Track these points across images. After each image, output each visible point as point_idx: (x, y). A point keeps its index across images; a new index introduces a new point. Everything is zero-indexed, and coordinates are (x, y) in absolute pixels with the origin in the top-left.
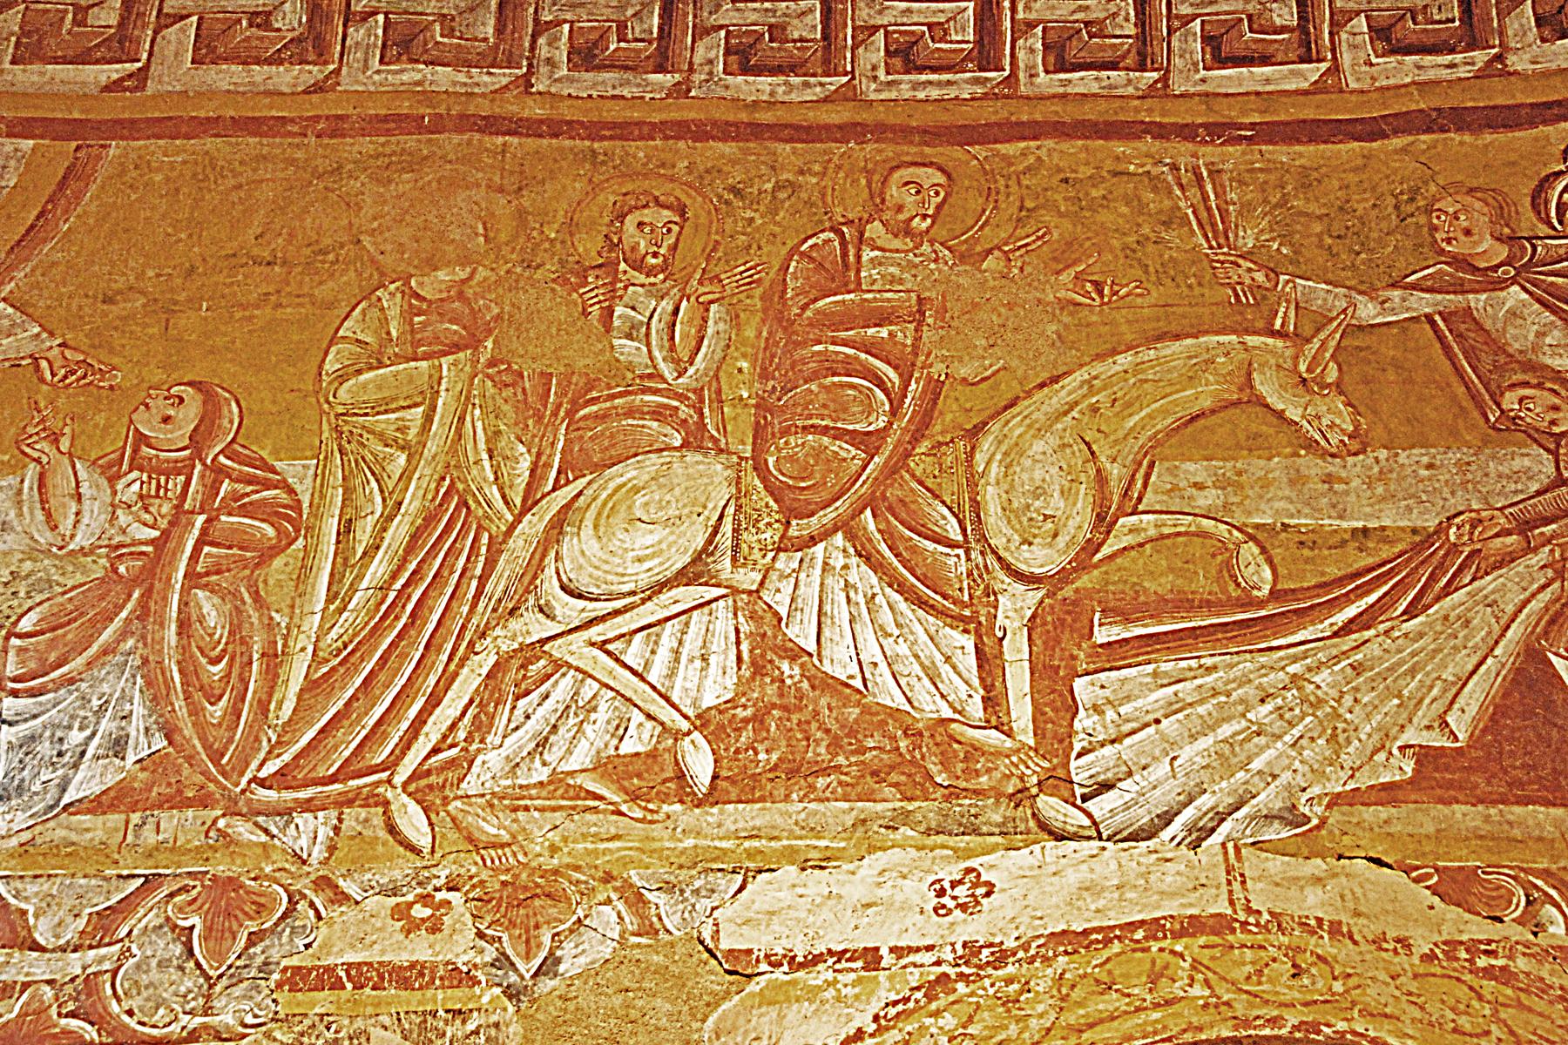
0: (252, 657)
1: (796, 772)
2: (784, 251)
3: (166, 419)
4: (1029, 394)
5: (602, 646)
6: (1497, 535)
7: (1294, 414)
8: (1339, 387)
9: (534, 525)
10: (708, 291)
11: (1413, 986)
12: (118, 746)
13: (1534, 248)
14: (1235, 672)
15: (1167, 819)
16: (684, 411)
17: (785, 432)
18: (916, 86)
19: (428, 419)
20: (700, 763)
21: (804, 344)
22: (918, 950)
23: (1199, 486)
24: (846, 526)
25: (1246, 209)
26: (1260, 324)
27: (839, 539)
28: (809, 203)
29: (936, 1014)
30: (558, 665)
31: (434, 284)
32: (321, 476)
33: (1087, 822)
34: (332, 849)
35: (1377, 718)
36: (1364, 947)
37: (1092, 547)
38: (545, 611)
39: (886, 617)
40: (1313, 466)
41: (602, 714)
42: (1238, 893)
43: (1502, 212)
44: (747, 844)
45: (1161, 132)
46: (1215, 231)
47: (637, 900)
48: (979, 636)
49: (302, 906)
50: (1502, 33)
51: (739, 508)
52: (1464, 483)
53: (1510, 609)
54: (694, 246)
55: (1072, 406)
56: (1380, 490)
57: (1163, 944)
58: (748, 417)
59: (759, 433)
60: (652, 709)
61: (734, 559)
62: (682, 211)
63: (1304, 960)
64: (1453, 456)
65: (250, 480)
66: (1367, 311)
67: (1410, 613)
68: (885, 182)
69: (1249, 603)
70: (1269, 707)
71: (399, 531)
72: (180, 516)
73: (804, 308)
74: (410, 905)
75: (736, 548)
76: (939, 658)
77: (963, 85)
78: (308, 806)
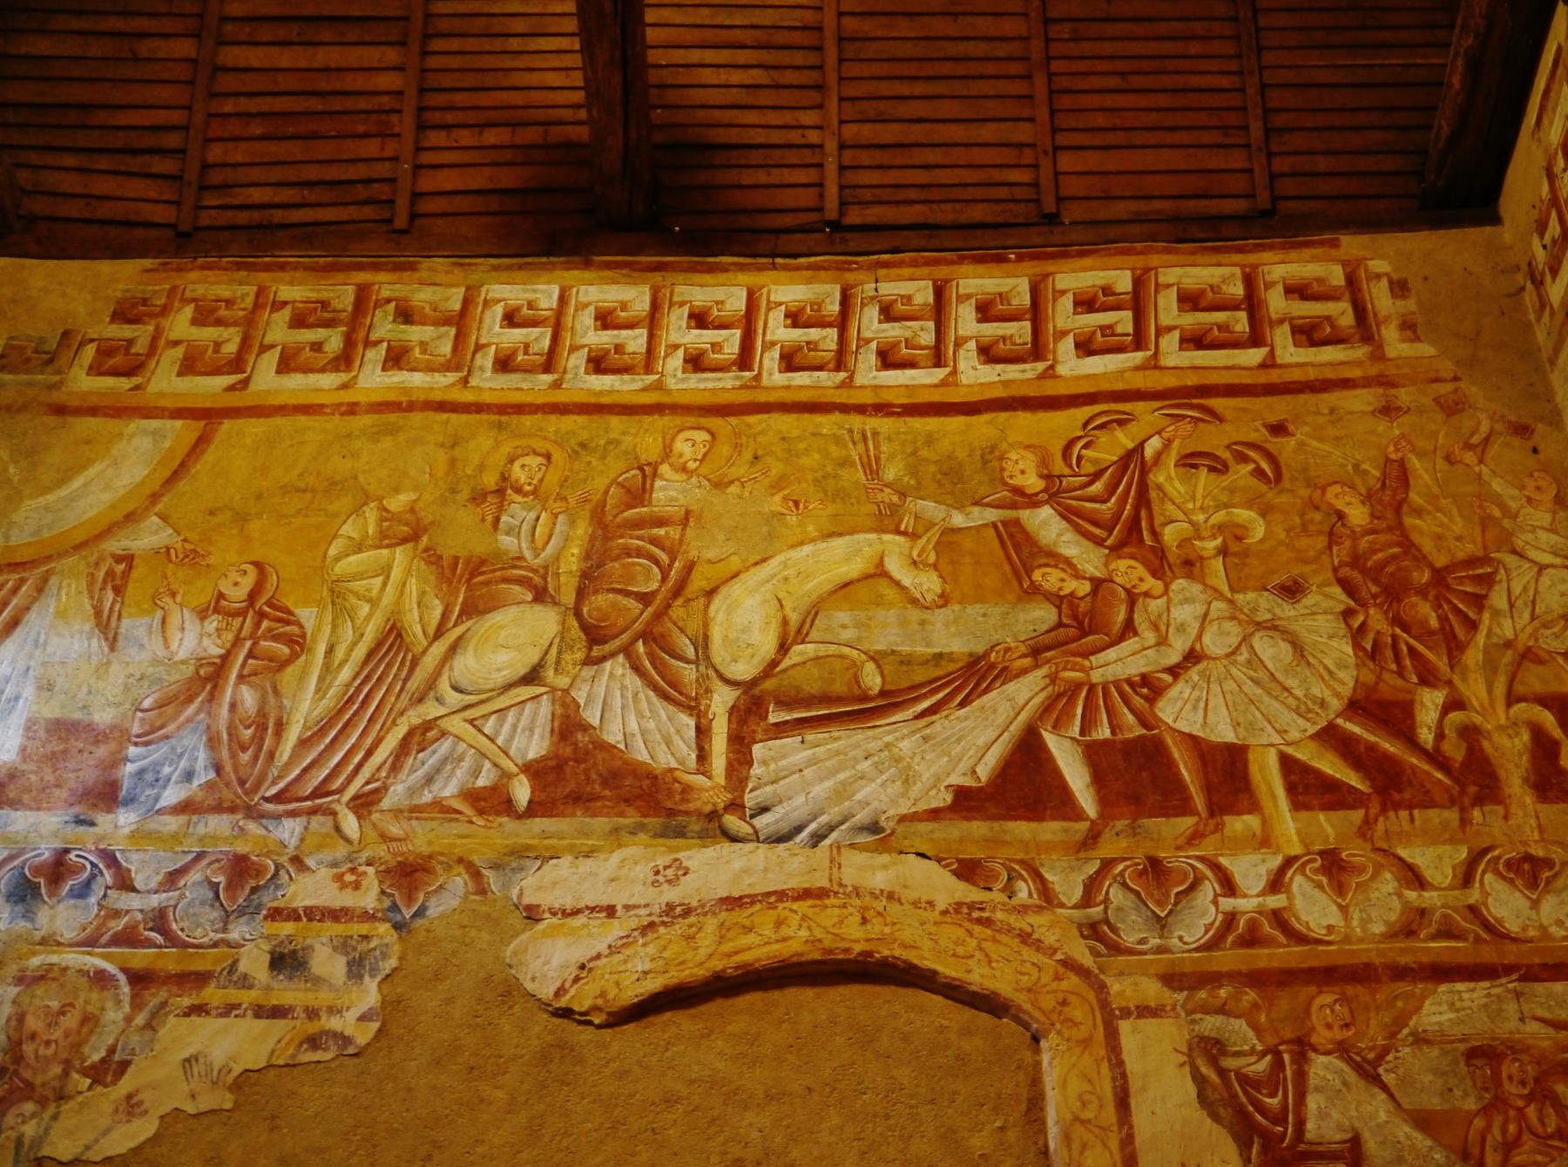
0: (268, 724)
1: (580, 800)
2: (607, 481)
3: (236, 584)
4: (747, 569)
5: (471, 722)
7: (906, 582)
8: (935, 566)
9: (439, 648)
10: (558, 506)
11: (933, 929)
12: (189, 776)
14: (853, 740)
15: (799, 829)
16: (537, 580)
17: (596, 592)
18: (700, 380)
19: (385, 584)
20: (522, 792)
21: (611, 539)
22: (638, 907)
23: (844, 626)
24: (627, 651)
25: (892, 456)
26: (892, 527)
27: (621, 658)
28: (626, 453)
29: (644, 945)
30: (443, 734)
31: (397, 503)
32: (320, 618)
33: (750, 831)
34: (302, 840)
35: (934, 769)
36: (907, 906)
37: (774, 663)
38: (439, 700)
39: (644, 706)
40: (914, 614)
41: (466, 764)
42: (835, 876)
43: (1044, 462)
44: (546, 842)
45: (845, 409)
47: (476, 874)
48: (698, 717)
49: (282, 873)
50: (1054, 352)
51: (562, 638)
52: (1003, 627)
53: (1021, 702)
54: (553, 478)
56: (953, 629)
57: (788, 905)
58: (574, 582)
59: (581, 593)
60: (499, 761)
61: (556, 670)
62: (548, 457)
63: (870, 914)
64: (999, 610)
65: (279, 620)
66: (958, 520)
67: (962, 705)
68: (673, 439)
69: (865, 698)
70: (869, 762)
71: (360, 652)
72: (238, 641)
73: (616, 516)
74: (343, 874)
75: (558, 662)
76: (672, 730)
77: (729, 380)
78: (293, 814)
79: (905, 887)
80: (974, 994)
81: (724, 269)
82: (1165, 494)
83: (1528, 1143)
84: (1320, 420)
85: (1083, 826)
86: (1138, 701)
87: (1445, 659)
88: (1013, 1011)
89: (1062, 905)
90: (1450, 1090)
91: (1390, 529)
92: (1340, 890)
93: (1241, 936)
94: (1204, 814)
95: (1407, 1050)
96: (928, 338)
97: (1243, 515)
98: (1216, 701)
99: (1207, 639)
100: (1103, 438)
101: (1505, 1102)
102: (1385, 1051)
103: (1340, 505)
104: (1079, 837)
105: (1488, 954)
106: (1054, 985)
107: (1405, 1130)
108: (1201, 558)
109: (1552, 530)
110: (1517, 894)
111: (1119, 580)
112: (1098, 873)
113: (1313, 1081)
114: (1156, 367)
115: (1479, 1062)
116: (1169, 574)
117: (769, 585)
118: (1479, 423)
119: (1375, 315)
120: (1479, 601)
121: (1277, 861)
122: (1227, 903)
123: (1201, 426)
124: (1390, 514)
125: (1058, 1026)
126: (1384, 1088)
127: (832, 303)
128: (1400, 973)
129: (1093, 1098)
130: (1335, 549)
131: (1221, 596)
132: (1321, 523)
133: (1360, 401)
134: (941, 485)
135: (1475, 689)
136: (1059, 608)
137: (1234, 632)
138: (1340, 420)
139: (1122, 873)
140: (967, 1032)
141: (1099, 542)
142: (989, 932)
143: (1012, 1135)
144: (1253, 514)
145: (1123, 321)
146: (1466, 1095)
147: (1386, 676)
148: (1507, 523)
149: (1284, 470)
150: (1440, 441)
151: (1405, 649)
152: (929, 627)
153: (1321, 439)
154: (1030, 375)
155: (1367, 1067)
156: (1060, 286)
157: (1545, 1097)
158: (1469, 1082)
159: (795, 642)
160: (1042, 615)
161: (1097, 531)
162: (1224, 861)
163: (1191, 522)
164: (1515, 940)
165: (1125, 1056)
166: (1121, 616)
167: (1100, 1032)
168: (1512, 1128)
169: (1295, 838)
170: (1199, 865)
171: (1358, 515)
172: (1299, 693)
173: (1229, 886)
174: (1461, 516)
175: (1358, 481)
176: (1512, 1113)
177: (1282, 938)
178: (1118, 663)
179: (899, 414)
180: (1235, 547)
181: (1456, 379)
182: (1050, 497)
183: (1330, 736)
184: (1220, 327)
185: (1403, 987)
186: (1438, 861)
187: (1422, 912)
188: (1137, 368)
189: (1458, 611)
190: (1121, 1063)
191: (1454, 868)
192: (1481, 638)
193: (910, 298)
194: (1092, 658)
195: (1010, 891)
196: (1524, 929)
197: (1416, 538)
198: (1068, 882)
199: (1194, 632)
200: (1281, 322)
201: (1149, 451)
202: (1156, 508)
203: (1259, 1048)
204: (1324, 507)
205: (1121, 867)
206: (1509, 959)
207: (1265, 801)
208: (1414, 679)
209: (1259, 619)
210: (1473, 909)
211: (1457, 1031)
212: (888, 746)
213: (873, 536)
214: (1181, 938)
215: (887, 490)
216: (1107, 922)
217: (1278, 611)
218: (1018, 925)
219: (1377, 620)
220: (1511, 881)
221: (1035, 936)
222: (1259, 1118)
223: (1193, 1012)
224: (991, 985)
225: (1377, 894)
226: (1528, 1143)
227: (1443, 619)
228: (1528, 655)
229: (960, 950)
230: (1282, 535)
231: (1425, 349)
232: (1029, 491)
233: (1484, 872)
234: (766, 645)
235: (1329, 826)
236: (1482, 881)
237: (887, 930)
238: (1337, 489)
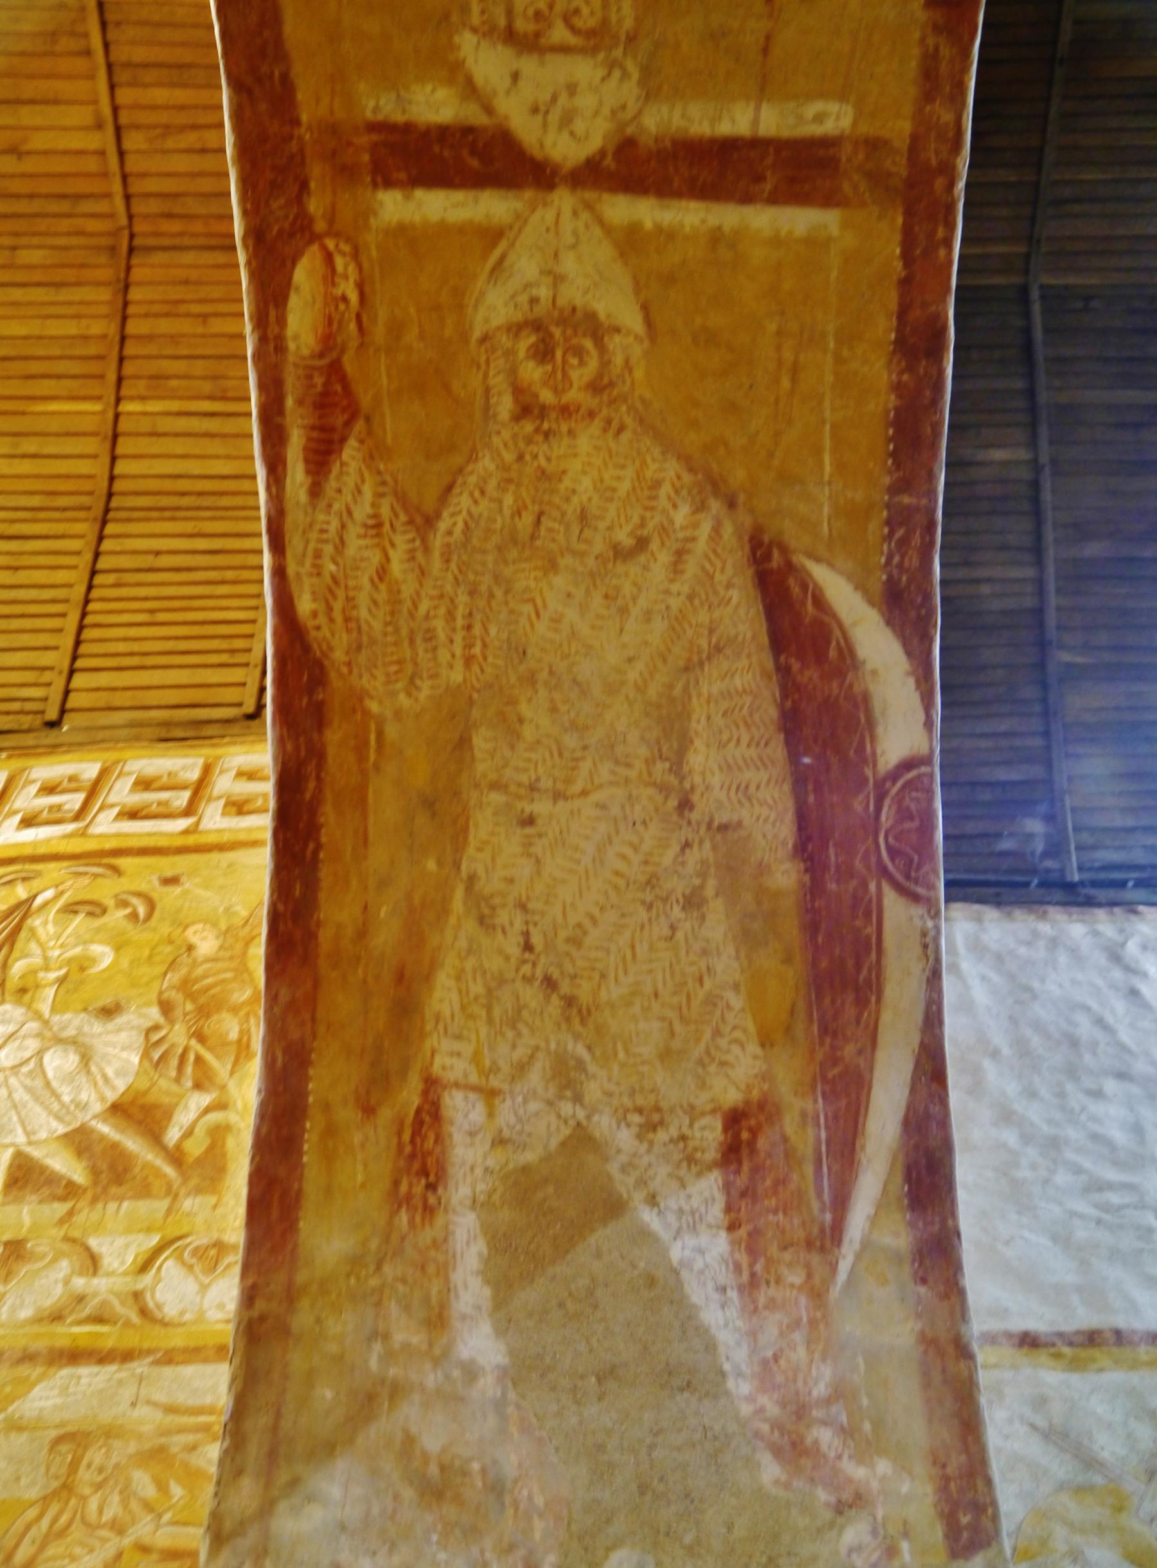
83: (77, 1531)
87: (229, 1067)
91: (231, 958)
105: (131, 1340)
115: (63, 1448)
123: (99, 881)
128: (28, 1357)
149: (157, 913)
151: (192, 1057)
153: (206, 887)
158: (43, 1470)
168: (64, 1519)
172: (66, 1099)
176: (73, 1502)
183: (80, 1141)
184: (159, 804)
185: (24, 1370)
196: (182, 1313)
200: (219, 798)
201: (39, 901)
208: (189, 1084)
210: (137, 1296)
217: (86, 1029)
219: (179, 1035)
220: (190, 1268)
227: (245, 1033)
238: (199, 926)
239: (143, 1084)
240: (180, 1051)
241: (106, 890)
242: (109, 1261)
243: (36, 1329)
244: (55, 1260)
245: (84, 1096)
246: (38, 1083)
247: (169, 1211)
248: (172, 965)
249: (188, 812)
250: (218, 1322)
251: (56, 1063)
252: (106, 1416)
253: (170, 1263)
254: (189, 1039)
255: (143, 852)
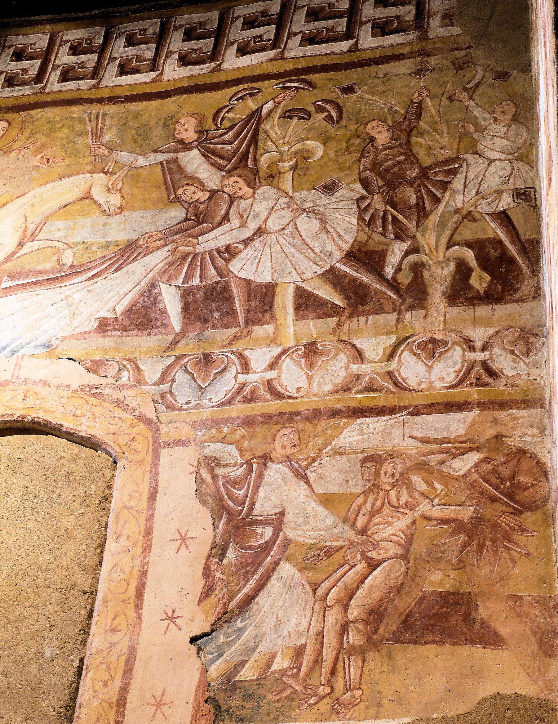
4: (12, 201)
6: (156, 240)
7: (101, 201)
8: (120, 191)
13: (208, 134)
18: (10, 92)
23: (59, 230)
26: (100, 170)
37: (13, 254)
43: (201, 123)
46: (96, 136)
50: (224, 55)
53: (151, 267)
55: (25, 204)
67: (116, 271)
79: (55, 377)
80: (82, 437)
81: (39, 23)
82: (268, 136)
83: (387, 510)
84: (376, 81)
85: (171, 338)
86: (220, 262)
87: (415, 223)
88: (103, 446)
89: (146, 384)
90: (347, 482)
91: (400, 146)
92: (311, 366)
93: (245, 396)
94: (242, 326)
95: (327, 459)
96: (149, 55)
97: (312, 144)
98: (266, 258)
99: (270, 222)
100: (240, 105)
101: (378, 487)
102: (314, 460)
103: (373, 133)
104: (166, 344)
105: (393, 401)
106: (129, 430)
107: (314, 506)
108: (280, 173)
109: (505, 138)
110: (421, 363)
111: (226, 190)
112: (172, 364)
113: (266, 479)
114: (282, 58)
115: (369, 464)
116: (258, 184)
117: (23, 209)
118: (476, 74)
119: (429, 11)
120: (444, 186)
121: (279, 350)
122: (242, 378)
123: (301, 91)
124: (403, 137)
125: (127, 454)
126: (308, 482)
127: (98, 38)
128: (335, 413)
129: (137, 494)
130: (363, 160)
131: (285, 194)
132: (359, 145)
133: (403, 67)
134: (135, 141)
135: (428, 239)
136: (187, 209)
137: (287, 215)
138: (389, 80)
139: (186, 364)
140: (76, 460)
141: (220, 168)
142: (98, 401)
143: (87, 517)
144: (318, 144)
145: (268, 32)
146: (357, 484)
147: (375, 236)
148: (476, 136)
149: (344, 115)
150: (448, 87)
151: (390, 218)
152: (108, 227)
153: (373, 94)
154: (205, 71)
155: (301, 470)
156: (237, 14)
157: (404, 483)
158: (360, 476)
159: (28, 241)
160: (177, 214)
161: (222, 162)
162: (247, 353)
163: (280, 152)
164: (411, 391)
165: (160, 470)
166: (222, 213)
167: (149, 458)
168: (379, 503)
169: (292, 337)
170: (232, 356)
171: (383, 137)
172: (317, 250)
173: (246, 367)
174: (448, 133)
175: (389, 117)
176: (381, 494)
177: (269, 397)
178: (216, 239)
179: (122, 102)
180: (301, 165)
181: (469, 47)
182: (199, 143)
184: (328, 30)
185: (335, 421)
186: (374, 346)
187: (358, 377)
188: (270, 60)
189: (430, 192)
190: (157, 473)
191: (385, 349)
192: (440, 209)
193: (145, 30)
194: (200, 238)
195: (117, 378)
196: (419, 384)
197: (415, 149)
198: (152, 371)
199: (263, 217)
200: (367, 22)
201: (265, 111)
202: (260, 145)
203: (240, 462)
204: (364, 135)
205: (186, 360)
206: (406, 403)
207: (279, 316)
208: (392, 236)
209: (305, 207)
211: (361, 447)
212: (67, 297)
213: (89, 175)
214: (210, 400)
215: (102, 148)
216: (171, 392)
217: (318, 202)
218: (116, 396)
219: (378, 202)
220: (418, 356)
221: (125, 403)
222: (229, 502)
223: (205, 442)
224: (92, 432)
225: (333, 367)
226: (387, 510)
227: (420, 199)
228: (469, 217)
229: (79, 413)
230: (332, 154)
231: (456, 30)
232: (187, 142)
233: (403, 351)
234: (11, 244)
235: (314, 328)
236: (400, 356)
237: (37, 402)
238: (375, 123)
239: (363, 237)
240: (382, 213)
241: (308, 99)
242: (369, 353)
243: (336, 396)
244: (336, 354)
245: (328, 248)
246: (298, 241)
247: (398, 321)
248: (363, 153)
249: (348, 35)
250: (442, 388)
251: (305, 226)
252: (388, 445)
253: (406, 353)
254: (386, 204)
255: (325, 68)
